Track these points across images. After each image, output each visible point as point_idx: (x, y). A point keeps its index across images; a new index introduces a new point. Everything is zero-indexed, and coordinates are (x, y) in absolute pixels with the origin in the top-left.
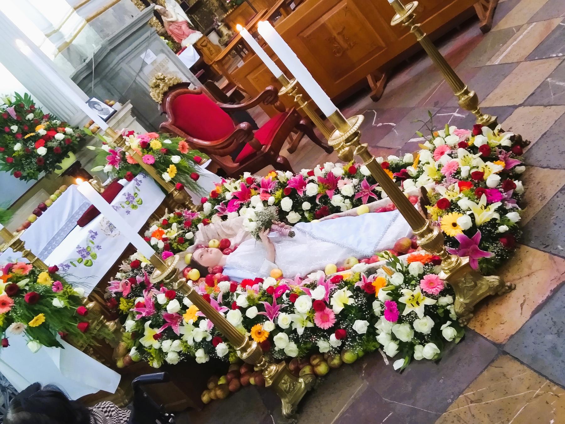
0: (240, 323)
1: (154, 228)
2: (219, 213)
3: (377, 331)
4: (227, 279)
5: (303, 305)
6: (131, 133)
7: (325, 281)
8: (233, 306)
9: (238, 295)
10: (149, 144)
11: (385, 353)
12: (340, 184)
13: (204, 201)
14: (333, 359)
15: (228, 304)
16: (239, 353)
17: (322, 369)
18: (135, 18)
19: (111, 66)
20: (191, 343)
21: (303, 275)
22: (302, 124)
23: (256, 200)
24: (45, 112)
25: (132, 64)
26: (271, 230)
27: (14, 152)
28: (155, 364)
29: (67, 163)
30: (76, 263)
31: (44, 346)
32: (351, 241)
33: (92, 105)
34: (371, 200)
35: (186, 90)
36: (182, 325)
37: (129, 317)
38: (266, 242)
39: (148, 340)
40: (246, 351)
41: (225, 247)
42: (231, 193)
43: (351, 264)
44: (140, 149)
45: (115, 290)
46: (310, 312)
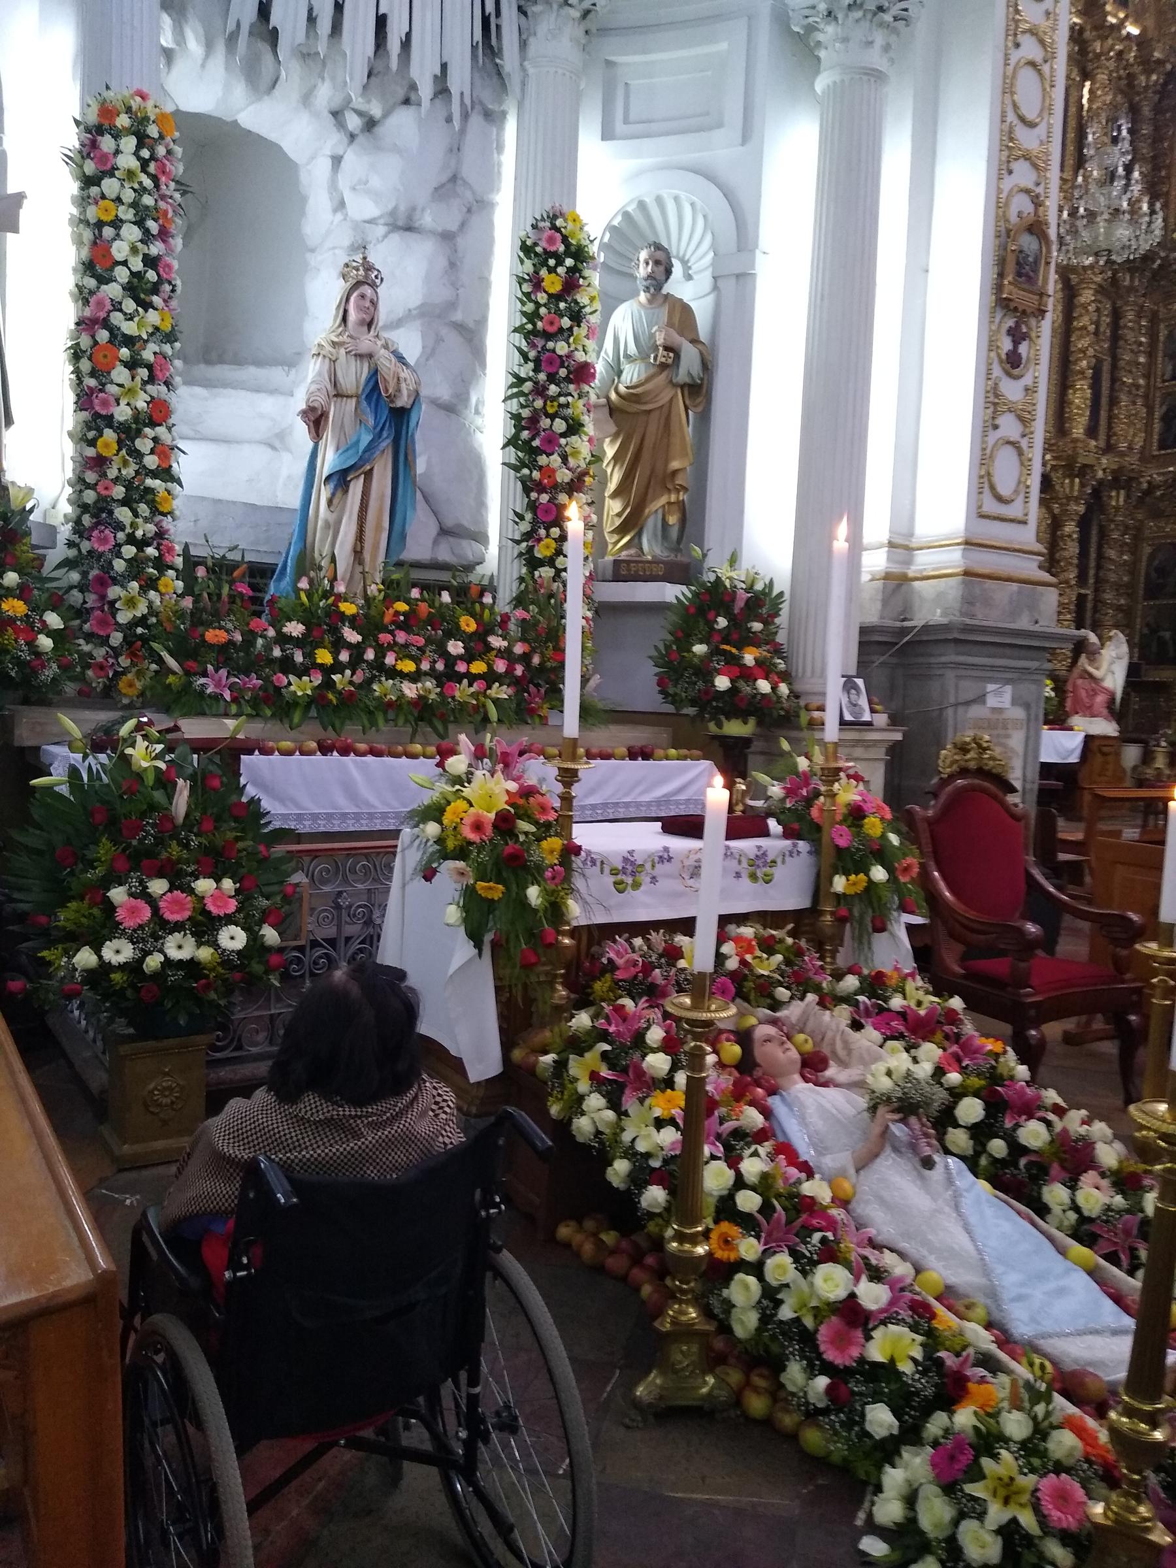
0: (715, 1193)
1: (747, 931)
2: (857, 1012)
3: (897, 1460)
4: (767, 1113)
5: (831, 1282)
6: (857, 778)
7: (902, 1290)
8: (733, 1161)
9: (755, 1154)
10: (864, 817)
11: (873, 1503)
12: (1088, 1179)
13: (851, 971)
14: (787, 1411)
15: (728, 1148)
16: (669, 1233)
17: (757, 1405)
18: (1036, 628)
19: (933, 660)
20: (627, 1137)
21: (880, 1239)
22: (1129, 1022)
23: (930, 1052)
24: (781, 638)
25: (964, 684)
26: (903, 1121)
27: (690, 651)
28: (555, 1110)
29: (735, 728)
30: (607, 870)
31: (462, 930)
32: (1009, 1281)
33: (849, 685)
34: (1112, 1258)
35: (1000, 794)
36: (641, 1101)
37: (592, 1010)
38: (877, 1129)
39: (578, 1068)
40: (681, 1243)
41: (813, 1066)
42: (905, 1003)
43: (971, 1314)
44: (844, 810)
45: (612, 955)
46: (829, 1304)
